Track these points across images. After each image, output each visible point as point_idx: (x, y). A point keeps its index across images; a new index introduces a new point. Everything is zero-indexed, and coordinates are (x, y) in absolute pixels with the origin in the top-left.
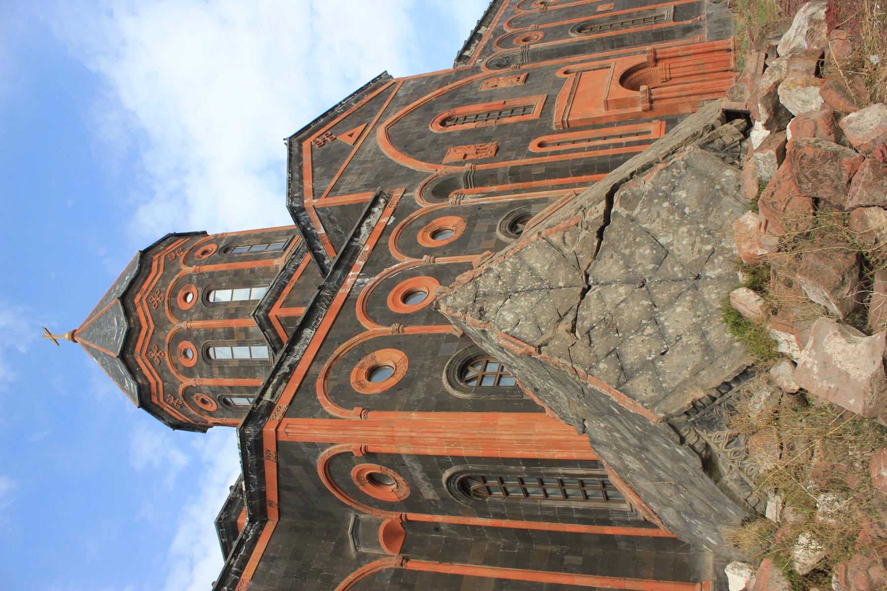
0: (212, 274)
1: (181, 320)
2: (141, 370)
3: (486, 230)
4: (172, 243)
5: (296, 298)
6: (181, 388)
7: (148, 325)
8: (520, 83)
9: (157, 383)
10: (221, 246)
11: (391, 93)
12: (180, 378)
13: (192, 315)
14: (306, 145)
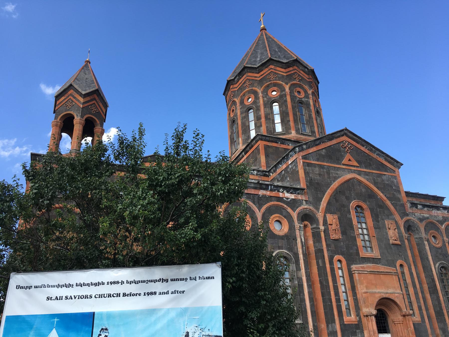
0: (286, 101)
1: (262, 93)
2: (241, 78)
3: (280, 245)
4: (304, 72)
5: (271, 150)
6: (236, 99)
7: (260, 77)
8: (391, 242)
9: (236, 88)
10: (303, 99)
11: (386, 171)
12: (239, 98)
13: (266, 97)
14: (344, 138)
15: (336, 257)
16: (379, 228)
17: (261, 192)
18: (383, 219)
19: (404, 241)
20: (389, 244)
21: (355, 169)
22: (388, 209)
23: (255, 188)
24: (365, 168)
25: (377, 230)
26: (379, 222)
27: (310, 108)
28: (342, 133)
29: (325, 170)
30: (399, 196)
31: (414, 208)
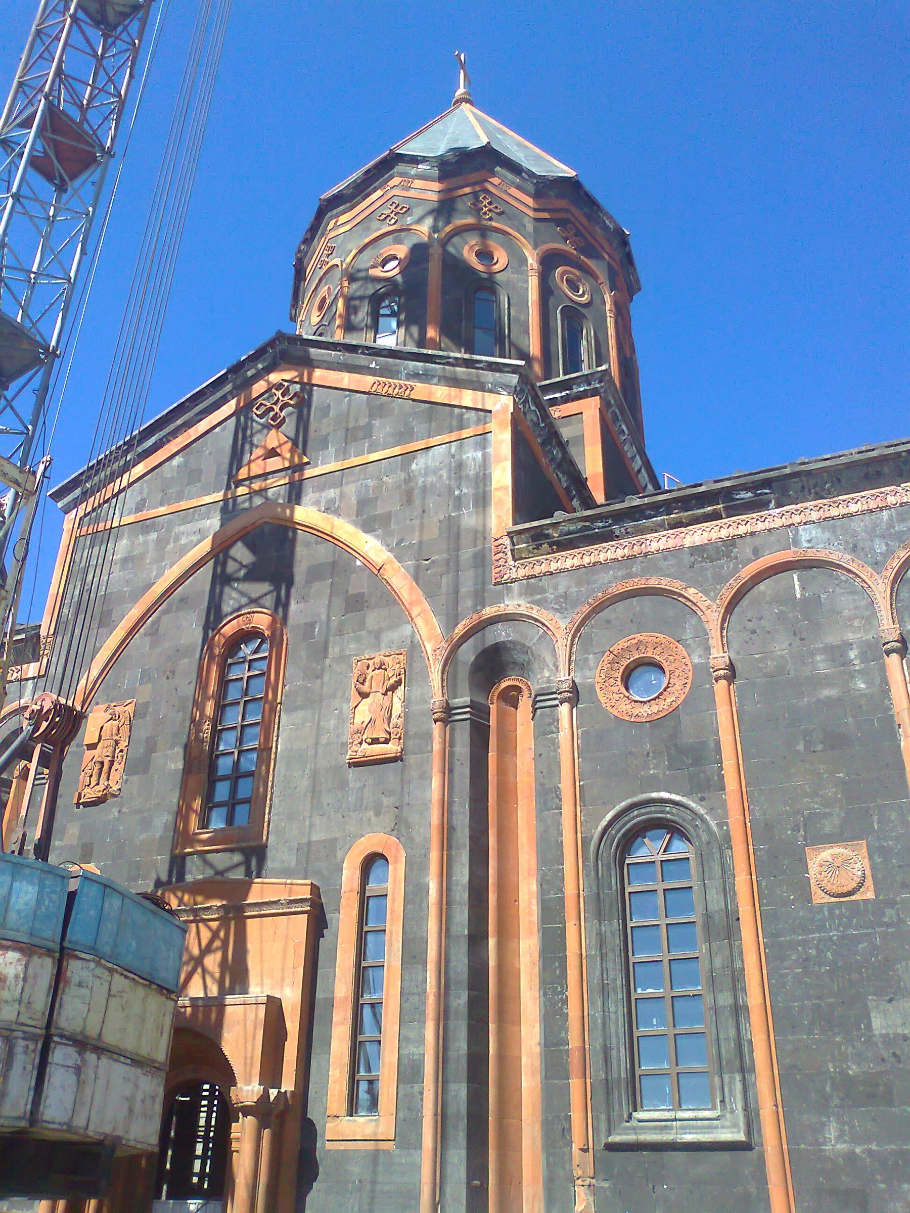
18: (343, 658)
19: (429, 736)
22: (389, 598)
24: (336, 460)
25: (298, 716)
29: (153, 536)
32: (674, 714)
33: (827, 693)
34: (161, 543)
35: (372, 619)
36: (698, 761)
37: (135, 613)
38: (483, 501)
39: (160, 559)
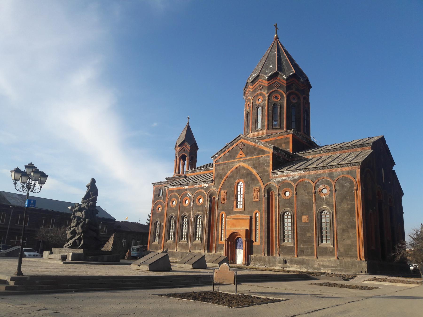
11: (264, 154)
15: (222, 212)
16: (248, 193)
17: (195, 186)
18: (252, 187)
20: (252, 202)
21: (243, 159)
22: (257, 180)
23: (193, 185)
26: (249, 189)
27: (264, 108)
28: (239, 138)
30: (268, 169)
31: (275, 176)
32: (289, 199)
33: (306, 198)
34: (227, 167)
35: (255, 182)
36: (292, 205)
37: (225, 178)
38: (269, 166)
39: (227, 170)
